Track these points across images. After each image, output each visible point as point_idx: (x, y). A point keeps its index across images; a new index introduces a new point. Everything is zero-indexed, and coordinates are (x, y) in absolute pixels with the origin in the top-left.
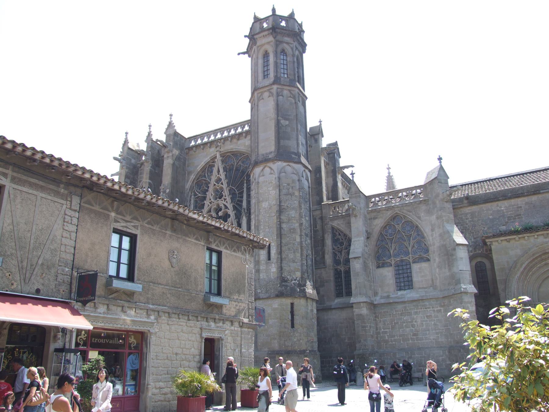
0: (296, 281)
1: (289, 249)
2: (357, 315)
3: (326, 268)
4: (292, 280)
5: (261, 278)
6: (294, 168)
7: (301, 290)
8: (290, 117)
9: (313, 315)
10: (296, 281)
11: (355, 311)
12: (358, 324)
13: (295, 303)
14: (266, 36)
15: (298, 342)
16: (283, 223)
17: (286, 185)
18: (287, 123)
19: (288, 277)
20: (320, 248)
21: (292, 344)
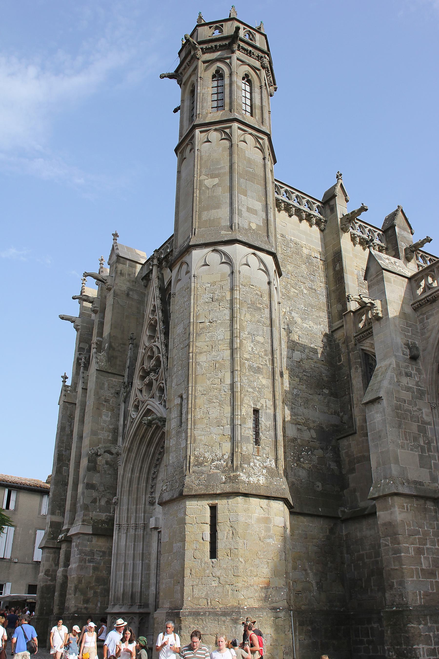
0: (222, 462)
1: (210, 401)
2: (384, 524)
3: (355, 433)
4: (213, 461)
5: (171, 462)
6: (225, 254)
7: (230, 477)
8: (222, 171)
9: (268, 529)
10: (222, 462)
11: (379, 516)
12: (386, 545)
13: (219, 507)
14: (190, 61)
15: (220, 590)
16: (201, 353)
17: (209, 285)
18: (216, 181)
19: (206, 455)
20: (347, 397)
21: (207, 594)
